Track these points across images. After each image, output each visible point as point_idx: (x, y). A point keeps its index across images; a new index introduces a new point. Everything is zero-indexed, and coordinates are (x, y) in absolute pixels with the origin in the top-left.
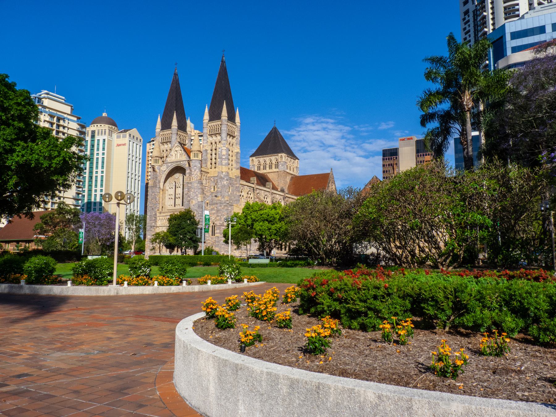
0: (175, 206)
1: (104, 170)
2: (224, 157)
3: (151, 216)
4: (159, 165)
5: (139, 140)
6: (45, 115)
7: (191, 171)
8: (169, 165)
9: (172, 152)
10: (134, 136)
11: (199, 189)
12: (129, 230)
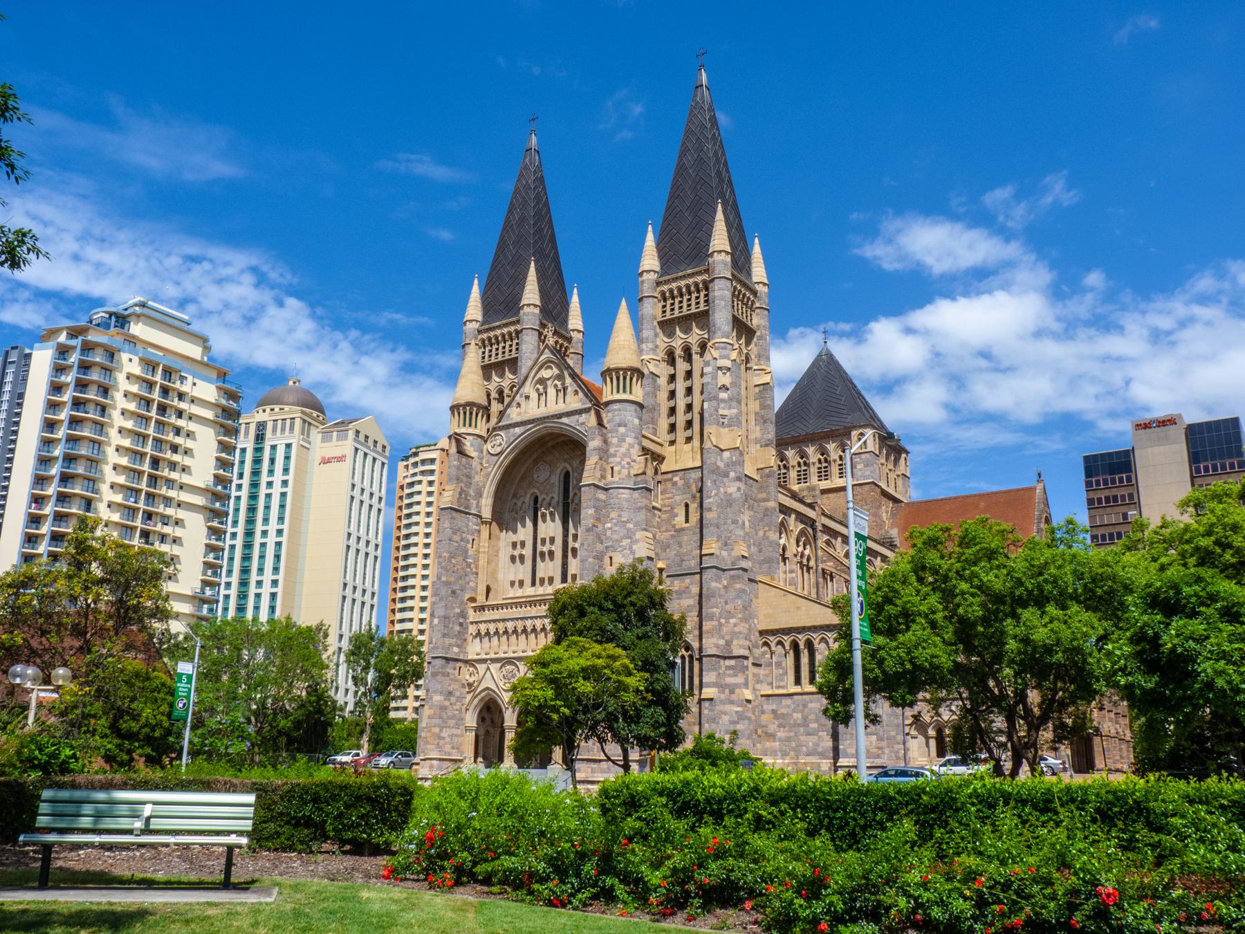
0: (533, 584)
1: (285, 527)
2: (723, 395)
3: (446, 617)
4: (477, 431)
5: (379, 448)
6: (131, 360)
7: (605, 441)
8: (518, 430)
9: (528, 383)
10: (367, 437)
11: (640, 509)
12: (356, 685)
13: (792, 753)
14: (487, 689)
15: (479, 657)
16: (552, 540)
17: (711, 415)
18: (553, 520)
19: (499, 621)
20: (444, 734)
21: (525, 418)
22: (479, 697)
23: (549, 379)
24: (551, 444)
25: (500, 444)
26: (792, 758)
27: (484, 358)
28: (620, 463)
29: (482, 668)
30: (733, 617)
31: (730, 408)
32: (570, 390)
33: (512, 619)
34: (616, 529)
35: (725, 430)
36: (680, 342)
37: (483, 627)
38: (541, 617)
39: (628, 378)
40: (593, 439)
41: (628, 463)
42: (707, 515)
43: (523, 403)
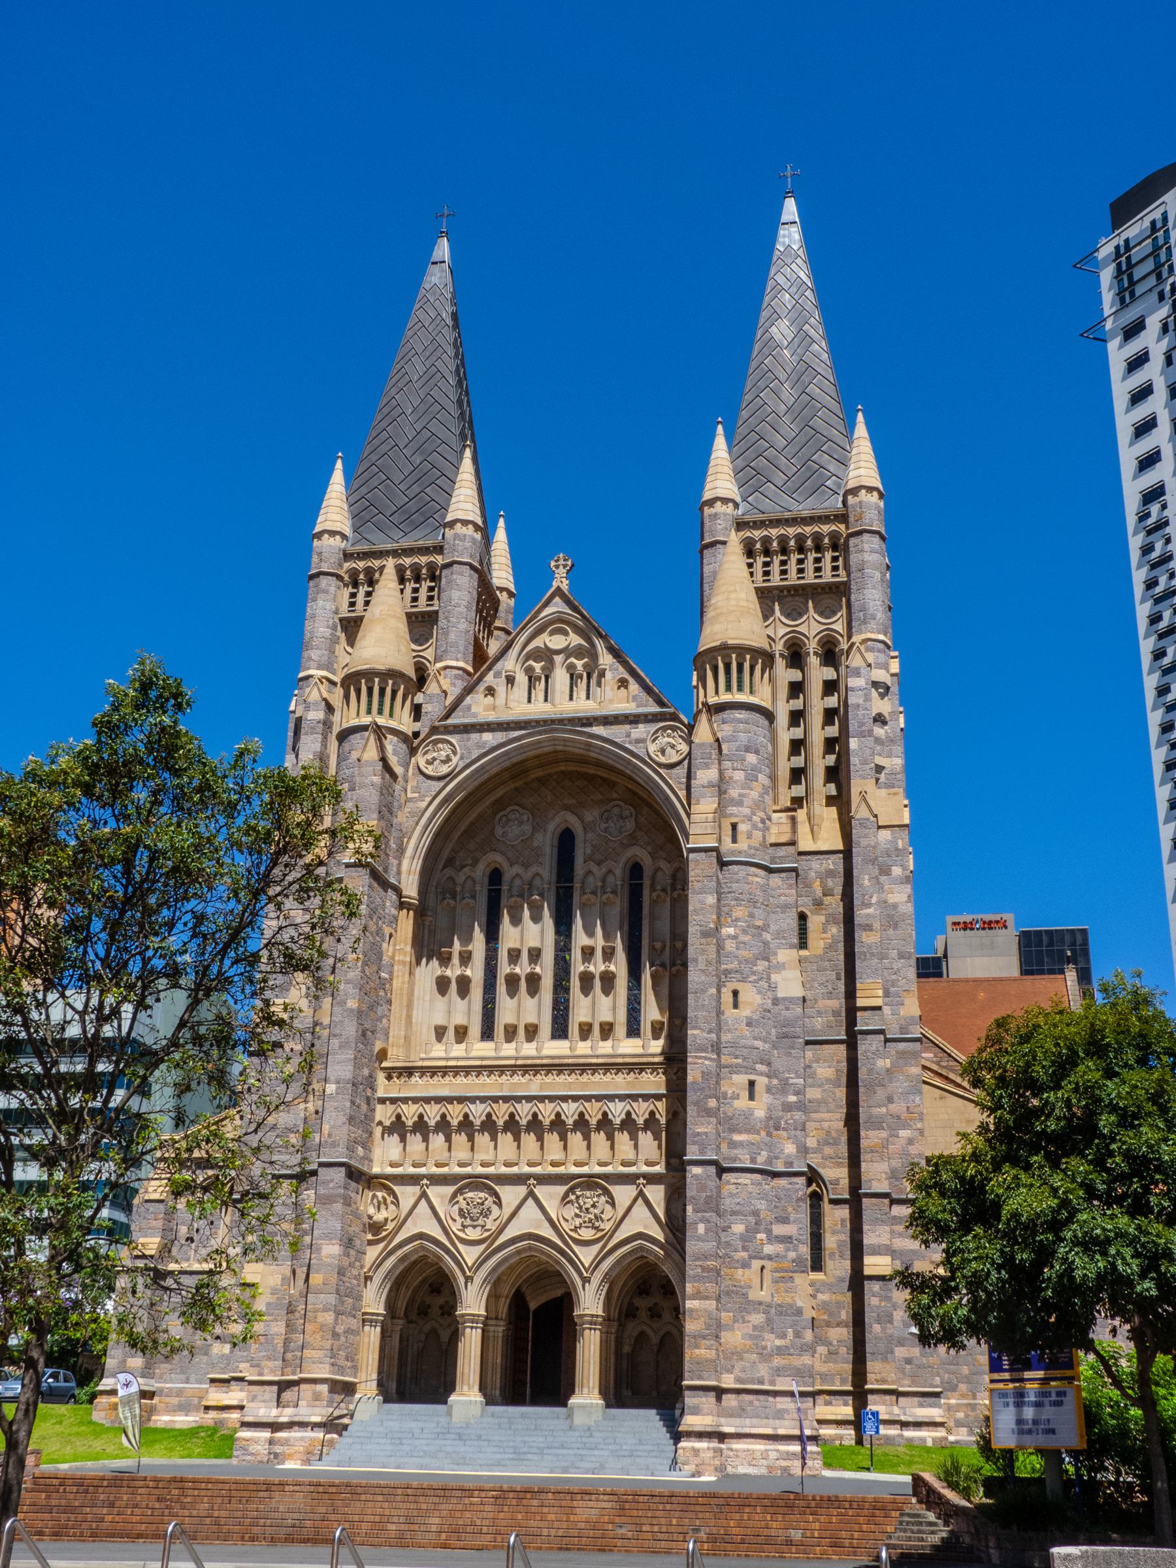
0: (487, 1033)
2: (879, 731)
8: (489, 738)
13: (963, 1387)
14: (421, 1236)
15: (398, 1171)
16: (535, 955)
17: (865, 762)
18: (536, 918)
19: (450, 1100)
20: (340, 1329)
21: (505, 716)
22: (400, 1253)
23: (558, 652)
24: (534, 775)
25: (447, 760)
26: (963, 1396)
27: (352, 604)
28: (750, 820)
29: (407, 1194)
30: (905, 1127)
31: (889, 756)
32: (608, 674)
33: (483, 1100)
34: (746, 938)
35: (883, 792)
36: (782, 631)
37: (410, 1112)
38: (646, 1097)
39: (747, 666)
40: (707, 766)
41: (763, 821)
42: (864, 939)
43: (501, 689)
